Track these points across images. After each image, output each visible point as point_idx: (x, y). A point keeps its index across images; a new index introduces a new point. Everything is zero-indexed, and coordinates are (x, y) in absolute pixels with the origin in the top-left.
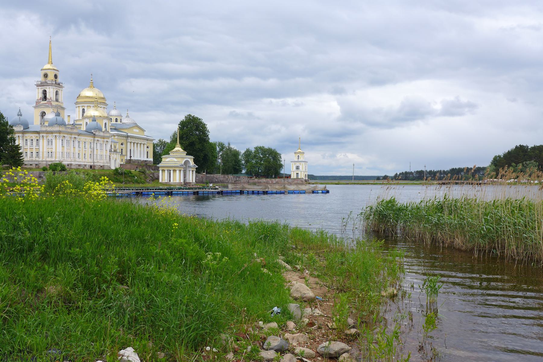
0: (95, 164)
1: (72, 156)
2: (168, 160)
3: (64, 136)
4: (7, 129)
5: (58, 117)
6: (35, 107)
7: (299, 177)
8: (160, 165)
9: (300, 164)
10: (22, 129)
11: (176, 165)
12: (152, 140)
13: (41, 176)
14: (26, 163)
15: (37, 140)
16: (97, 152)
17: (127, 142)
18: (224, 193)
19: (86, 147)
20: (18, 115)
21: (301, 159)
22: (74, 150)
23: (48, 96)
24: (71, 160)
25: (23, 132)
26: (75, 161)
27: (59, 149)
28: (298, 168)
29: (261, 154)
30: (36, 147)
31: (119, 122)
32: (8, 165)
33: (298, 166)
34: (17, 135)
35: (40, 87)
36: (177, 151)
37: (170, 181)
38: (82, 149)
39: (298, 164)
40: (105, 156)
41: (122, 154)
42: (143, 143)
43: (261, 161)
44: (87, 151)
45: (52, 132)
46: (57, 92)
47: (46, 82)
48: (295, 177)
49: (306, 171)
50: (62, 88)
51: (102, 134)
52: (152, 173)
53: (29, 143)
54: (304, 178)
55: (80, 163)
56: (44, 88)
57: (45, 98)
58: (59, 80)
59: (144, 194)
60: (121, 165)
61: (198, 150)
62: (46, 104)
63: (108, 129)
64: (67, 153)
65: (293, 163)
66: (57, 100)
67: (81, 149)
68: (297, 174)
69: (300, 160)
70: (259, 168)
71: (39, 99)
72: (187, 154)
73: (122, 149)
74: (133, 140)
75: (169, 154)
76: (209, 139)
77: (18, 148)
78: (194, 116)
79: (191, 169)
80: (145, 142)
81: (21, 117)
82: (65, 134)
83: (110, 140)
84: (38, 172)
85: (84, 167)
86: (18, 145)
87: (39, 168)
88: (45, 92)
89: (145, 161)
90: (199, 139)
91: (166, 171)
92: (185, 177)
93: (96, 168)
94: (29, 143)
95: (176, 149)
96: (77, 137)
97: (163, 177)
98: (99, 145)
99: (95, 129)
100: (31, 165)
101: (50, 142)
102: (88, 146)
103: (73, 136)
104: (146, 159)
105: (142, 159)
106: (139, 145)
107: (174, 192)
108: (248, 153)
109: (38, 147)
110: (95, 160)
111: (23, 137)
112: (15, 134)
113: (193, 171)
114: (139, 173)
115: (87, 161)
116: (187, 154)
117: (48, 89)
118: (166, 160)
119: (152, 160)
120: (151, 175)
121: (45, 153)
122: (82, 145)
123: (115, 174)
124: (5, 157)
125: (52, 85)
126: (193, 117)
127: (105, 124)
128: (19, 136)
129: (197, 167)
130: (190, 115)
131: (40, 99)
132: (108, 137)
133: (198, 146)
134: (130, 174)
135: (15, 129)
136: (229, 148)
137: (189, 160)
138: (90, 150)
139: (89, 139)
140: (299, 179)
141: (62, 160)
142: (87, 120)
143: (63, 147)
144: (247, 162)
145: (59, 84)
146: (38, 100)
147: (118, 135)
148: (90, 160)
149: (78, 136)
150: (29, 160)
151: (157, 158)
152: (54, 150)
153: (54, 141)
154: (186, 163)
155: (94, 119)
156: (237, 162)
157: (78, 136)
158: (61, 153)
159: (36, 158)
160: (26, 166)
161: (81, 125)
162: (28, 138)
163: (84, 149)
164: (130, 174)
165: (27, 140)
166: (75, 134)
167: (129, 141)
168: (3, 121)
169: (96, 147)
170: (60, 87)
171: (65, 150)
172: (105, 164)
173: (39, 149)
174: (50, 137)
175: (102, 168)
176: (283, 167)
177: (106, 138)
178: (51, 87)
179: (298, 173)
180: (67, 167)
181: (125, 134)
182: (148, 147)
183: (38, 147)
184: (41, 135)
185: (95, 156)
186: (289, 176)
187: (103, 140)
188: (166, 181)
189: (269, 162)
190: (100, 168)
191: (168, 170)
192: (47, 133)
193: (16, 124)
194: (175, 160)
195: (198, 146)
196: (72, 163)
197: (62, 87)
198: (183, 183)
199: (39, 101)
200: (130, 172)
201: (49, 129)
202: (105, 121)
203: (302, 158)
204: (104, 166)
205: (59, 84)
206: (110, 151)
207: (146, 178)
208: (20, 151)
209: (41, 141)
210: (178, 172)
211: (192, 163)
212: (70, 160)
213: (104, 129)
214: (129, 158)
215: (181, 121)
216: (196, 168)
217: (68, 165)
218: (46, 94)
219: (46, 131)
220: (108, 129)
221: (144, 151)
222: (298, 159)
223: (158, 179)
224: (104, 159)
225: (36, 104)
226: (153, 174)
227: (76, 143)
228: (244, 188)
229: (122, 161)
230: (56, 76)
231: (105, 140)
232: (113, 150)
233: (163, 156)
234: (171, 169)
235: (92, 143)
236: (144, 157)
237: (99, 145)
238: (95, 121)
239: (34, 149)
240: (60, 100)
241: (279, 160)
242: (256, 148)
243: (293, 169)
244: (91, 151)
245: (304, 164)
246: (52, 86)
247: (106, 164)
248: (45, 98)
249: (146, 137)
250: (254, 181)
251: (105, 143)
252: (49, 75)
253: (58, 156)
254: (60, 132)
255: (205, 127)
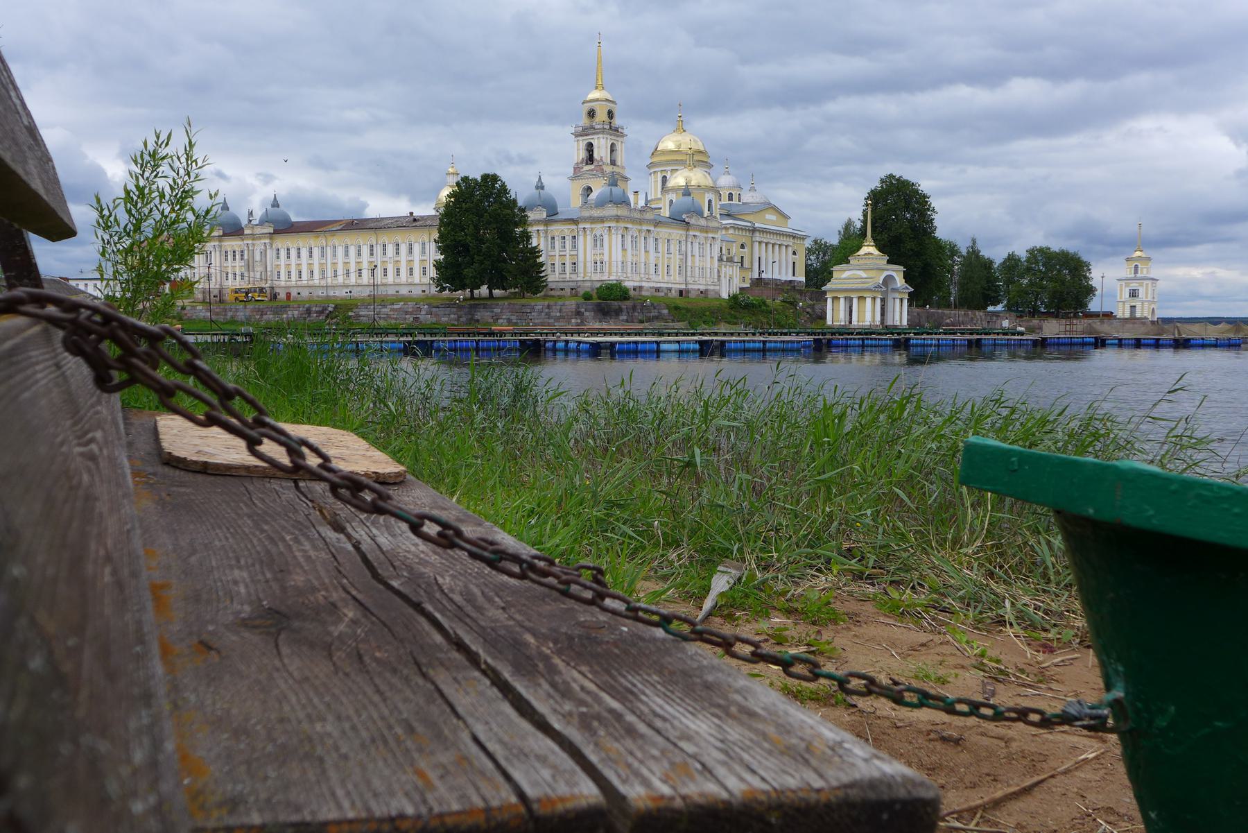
0: (690, 287)
1: (643, 271)
2: (846, 274)
3: (626, 228)
4: (514, 215)
5: (614, 188)
6: (573, 179)
7: (1138, 315)
8: (829, 286)
9: (1141, 285)
10: (544, 215)
11: (866, 285)
12: (803, 238)
13: (580, 312)
14: (551, 285)
15: (574, 237)
16: (693, 262)
17: (753, 242)
18: (1050, 345)
19: (672, 250)
20: (537, 188)
21: (1142, 273)
22: (647, 258)
23: (595, 155)
24: (641, 278)
25: (547, 222)
26: (649, 280)
27: (617, 255)
28: (1134, 294)
29: (1043, 266)
30: (572, 253)
31: (735, 201)
32: (517, 290)
33: (1134, 290)
34: (535, 228)
35: (581, 138)
36: (866, 254)
37: (850, 322)
38: (663, 256)
39: (1134, 285)
40: (708, 270)
41: (742, 265)
42: (785, 243)
43: (1042, 279)
44: (672, 260)
45: (601, 220)
46: (612, 145)
47: (592, 127)
48: (1127, 315)
49: (1154, 302)
50: (623, 137)
51: (702, 222)
52: (810, 305)
53: (557, 243)
54: (1150, 317)
55: (658, 285)
56: (589, 139)
57: (590, 159)
58: (617, 122)
59: (837, 346)
60: (741, 289)
61: (911, 253)
62: (592, 170)
63: (716, 212)
64: (632, 264)
65: (1123, 283)
66: (613, 163)
67: (660, 255)
68: (1133, 307)
69: (1139, 275)
70: (1037, 295)
71: (579, 162)
72: (889, 262)
73: (742, 257)
74: (766, 238)
75: (848, 262)
76: (934, 229)
77: (535, 252)
78: (901, 177)
79: (897, 295)
80: (790, 241)
81: (541, 191)
82: (628, 222)
83: (718, 236)
84: (573, 302)
85: (666, 294)
86: (536, 247)
87: (577, 295)
88: (590, 148)
89: (790, 281)
90: (911, 228)
91: (842, 301)
92: (883, 314)
93: (692, 295)
94: (557, 243)
95: (864, 250)
96: (652, 228)
97: (836, 315)
98: (696, 246)
99: (688, 212)
100: (562, 289)
101: (598, 241)
102: (674, 247)
103: (645, 228)
104: (790, 278)
105: (784, 278)
106: (777, 247)
107: (915, 341)
108: (1012, 262)
109: (575, 253)
110: (689, 279)
111: (546, 232)
112: (531, 225)
113: (901, 300)
114: (783, 304)
115: (671, 281)
116: (889, 262)
117: (596, 140)
118: (843, 276)
119: (803, 279)
120: (808, 310)
121: (589, 265)
122: (662, 247)
123: (731, 308)
124: (509, 272)
125: (603, 131)
126: (898, 180)
127: (710, 201)
128: (538, 230)
129: (912, 290)
130: (891, 176)
131: (582, 163)
132: (716, 230)
133: (909, 245)
134: (763, 308)
135: (532, 216)
136: (974, 251)
137: (894, 274)
138: (678, 256)
139: (677, 233)
140: (1138, 319)
141: (622, 278)
142: (673, 196)
143: (624, 249)
144: (1009, 281)
145: (617, 130)
146: (577, 163)
147: (735, 228)
148: (678, 279)
149: (655, 226)
150: (557, 280)
151: (818, 276)
152: (606, 258)
153: (606, 238)
154: (888, 280)
155: (687, 191)
156: (990, 280)
157: (655, 226)
158: (620, 264)
159: (572, 276)
160: (552, 293)
161: (661, 208)
162: (556, 234)
163: (666, 255)
164: (763, 308)
165: (553, 238)
166: (649, 222)
167: (758, 239)
168: (507, 198)
169: (692, 251)
170: (618, 136)
171: (629, 258)
172: (709, 287)
173: (577, 255)
174: (599, 229)
175: (703, 295)
176: (1098, 293)
177: (712, 232)
178: (601, 136)
179: (1135, 306)
180: (632, 293)
181: (749, 224)
182: (794, 253)
183: (575, 253)
184: (581, 226)
185: (689, 268)
186: (1109, 315)
187: (705, 235)
188: (843, 323)
189: (1063, 282)
190: (698, 295)
191: (845, 298)
192: (592, 223)
193: (532, 207)
194: (863, 274)
195: (909, 245)
196: (644, 284)
197: (623, 135)
198: (881, 327)
199: (580, 166)
200: (764, 303)
201: (597, 213)
202: (709, 196)
203: (1145, 270)
204: (707, 290)
205: (617, 130)
206: (720, 260)
207: (797, 315)
208: (541, 260)
209: (581, 239)
210: (869, 301)
211: (900, 281)
212: (638, 279)
213: (706, 213)
214: (757, 276)
215: (872, 191)
216: (910, 294)
217: (634, 289)
218: (593, 151)
219: (591, 217)
220: (716, 212)
221: (786, 260)
222: (1136, 272)
223: (823, 317)
224: (708, 276)
225: (574, 174)
226: (812, 307)
227: (651, 241)
228: (1091, 330)
229: (744, 281)
230: (611, 114)
231: (711, 235)
232: (725, 259)
233: (835, 268)
234: (852, 296)
235: (683, 243)
236: (787, 273)
237: (696, 246)
238: (689, 195)
239: (568, 256)
240: (619, 163)
241: (1086, 277)
242: (1031, 252)
243: (1121, 298)
244: (681, 259)
245: (1150, 285)
246: (603, 133)
247: (712, 288)
248: (590, 159)
249: (791, 231)
250: (1031, 324)
251: (709, 242)
252: (598, 112)
253: (614, 269)
254: (618, 219)
255: (927, 202)
